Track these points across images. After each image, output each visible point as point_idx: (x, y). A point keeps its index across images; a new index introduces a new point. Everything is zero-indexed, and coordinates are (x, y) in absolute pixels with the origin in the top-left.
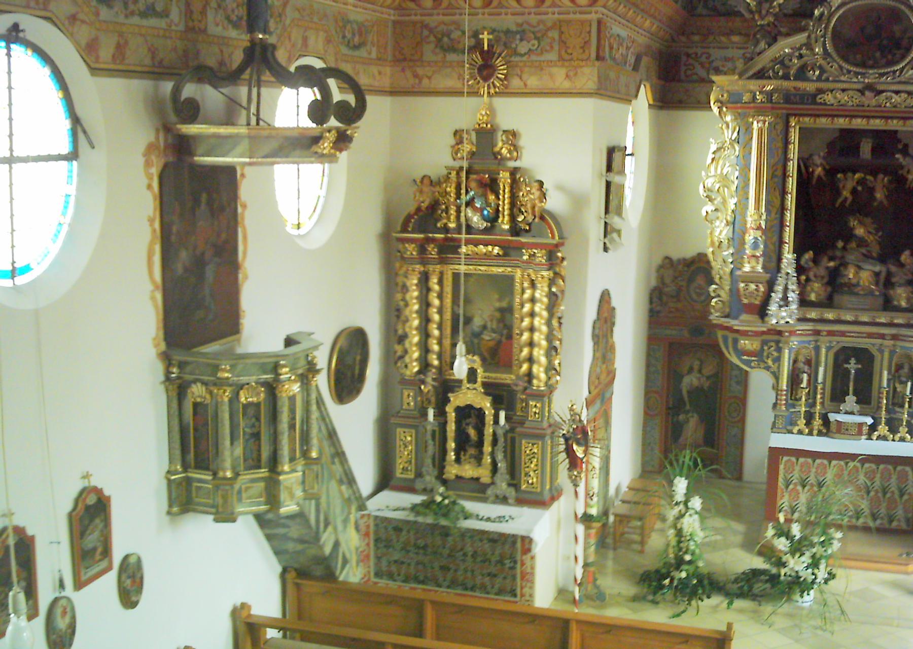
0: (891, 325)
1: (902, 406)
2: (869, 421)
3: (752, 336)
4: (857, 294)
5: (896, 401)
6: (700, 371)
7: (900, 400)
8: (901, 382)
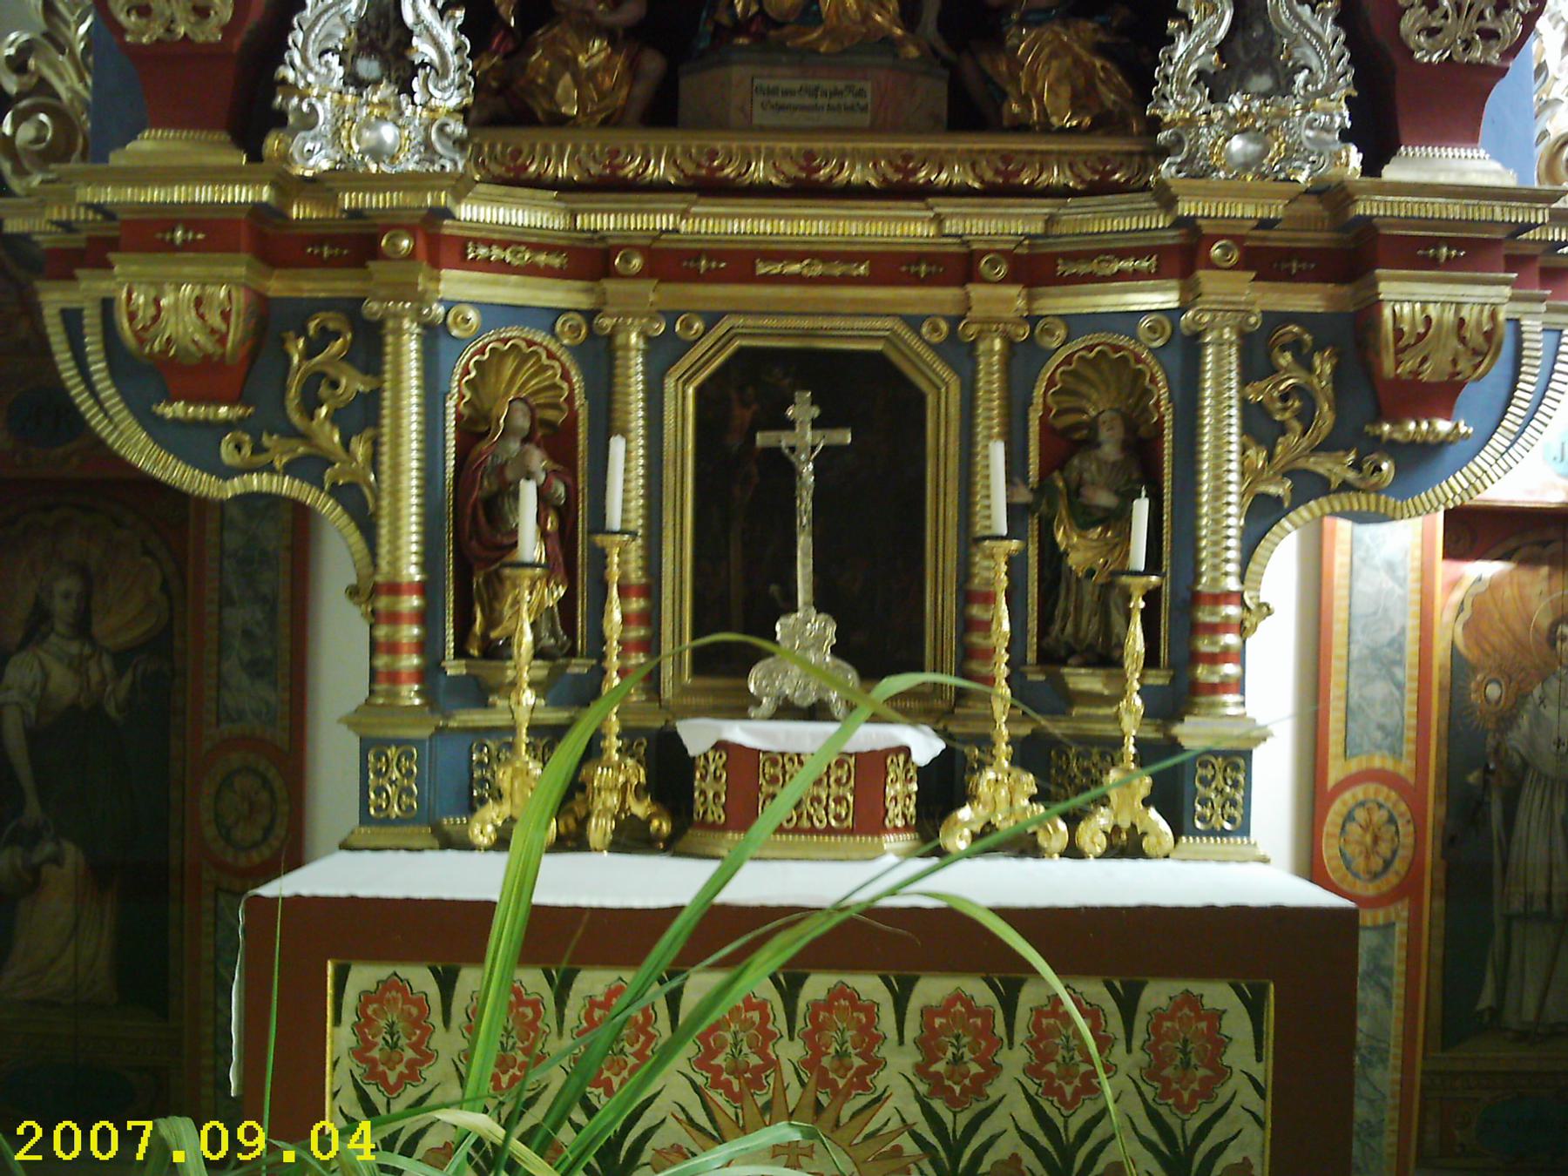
0: (1003, 190)
1: (1107, 658)
2: (925, 746)
3: (187, 246)
4: (806, 58)
5: (1064, 630)
6: (82, 627)
7: (1090, 627)
8: (1085, 518)
